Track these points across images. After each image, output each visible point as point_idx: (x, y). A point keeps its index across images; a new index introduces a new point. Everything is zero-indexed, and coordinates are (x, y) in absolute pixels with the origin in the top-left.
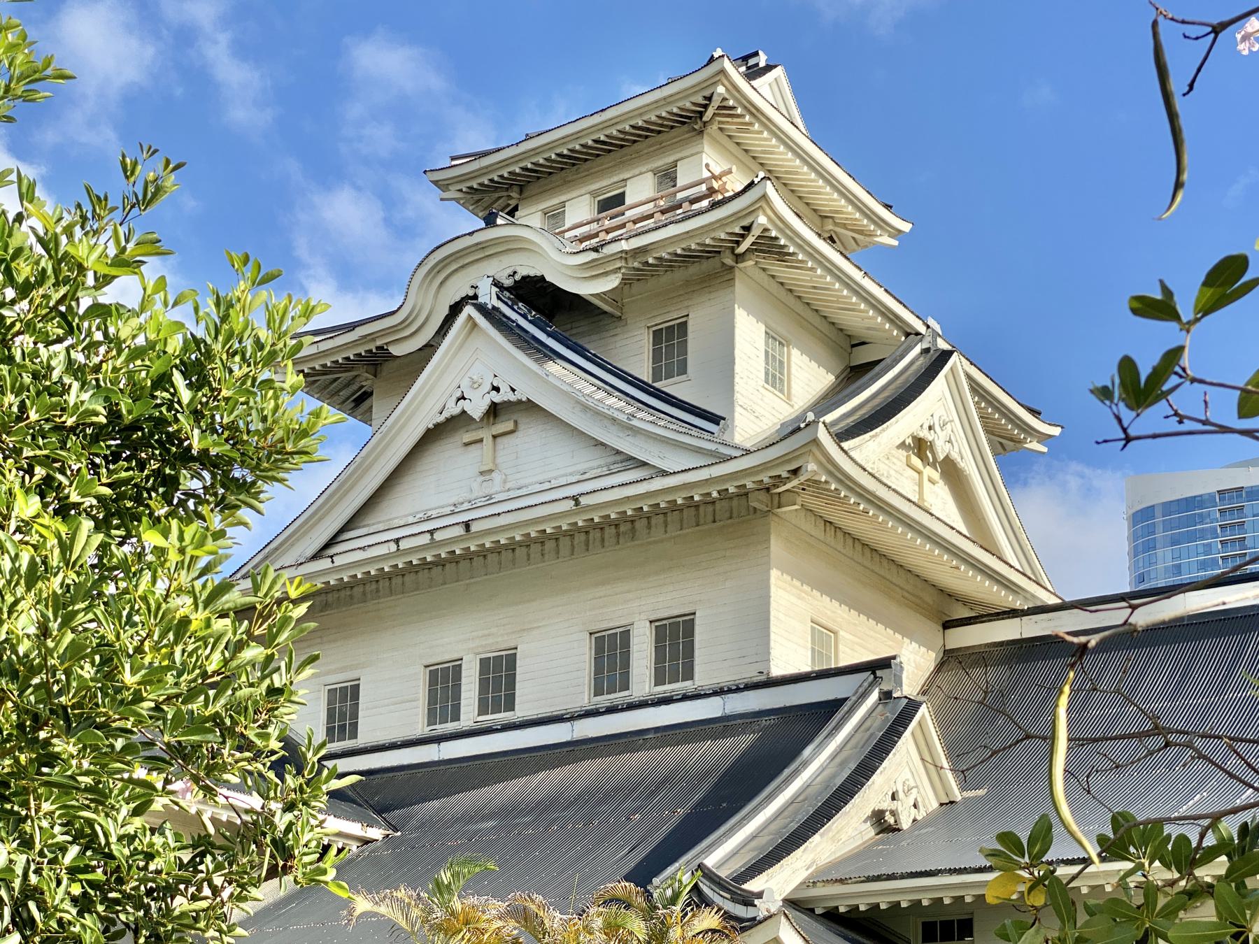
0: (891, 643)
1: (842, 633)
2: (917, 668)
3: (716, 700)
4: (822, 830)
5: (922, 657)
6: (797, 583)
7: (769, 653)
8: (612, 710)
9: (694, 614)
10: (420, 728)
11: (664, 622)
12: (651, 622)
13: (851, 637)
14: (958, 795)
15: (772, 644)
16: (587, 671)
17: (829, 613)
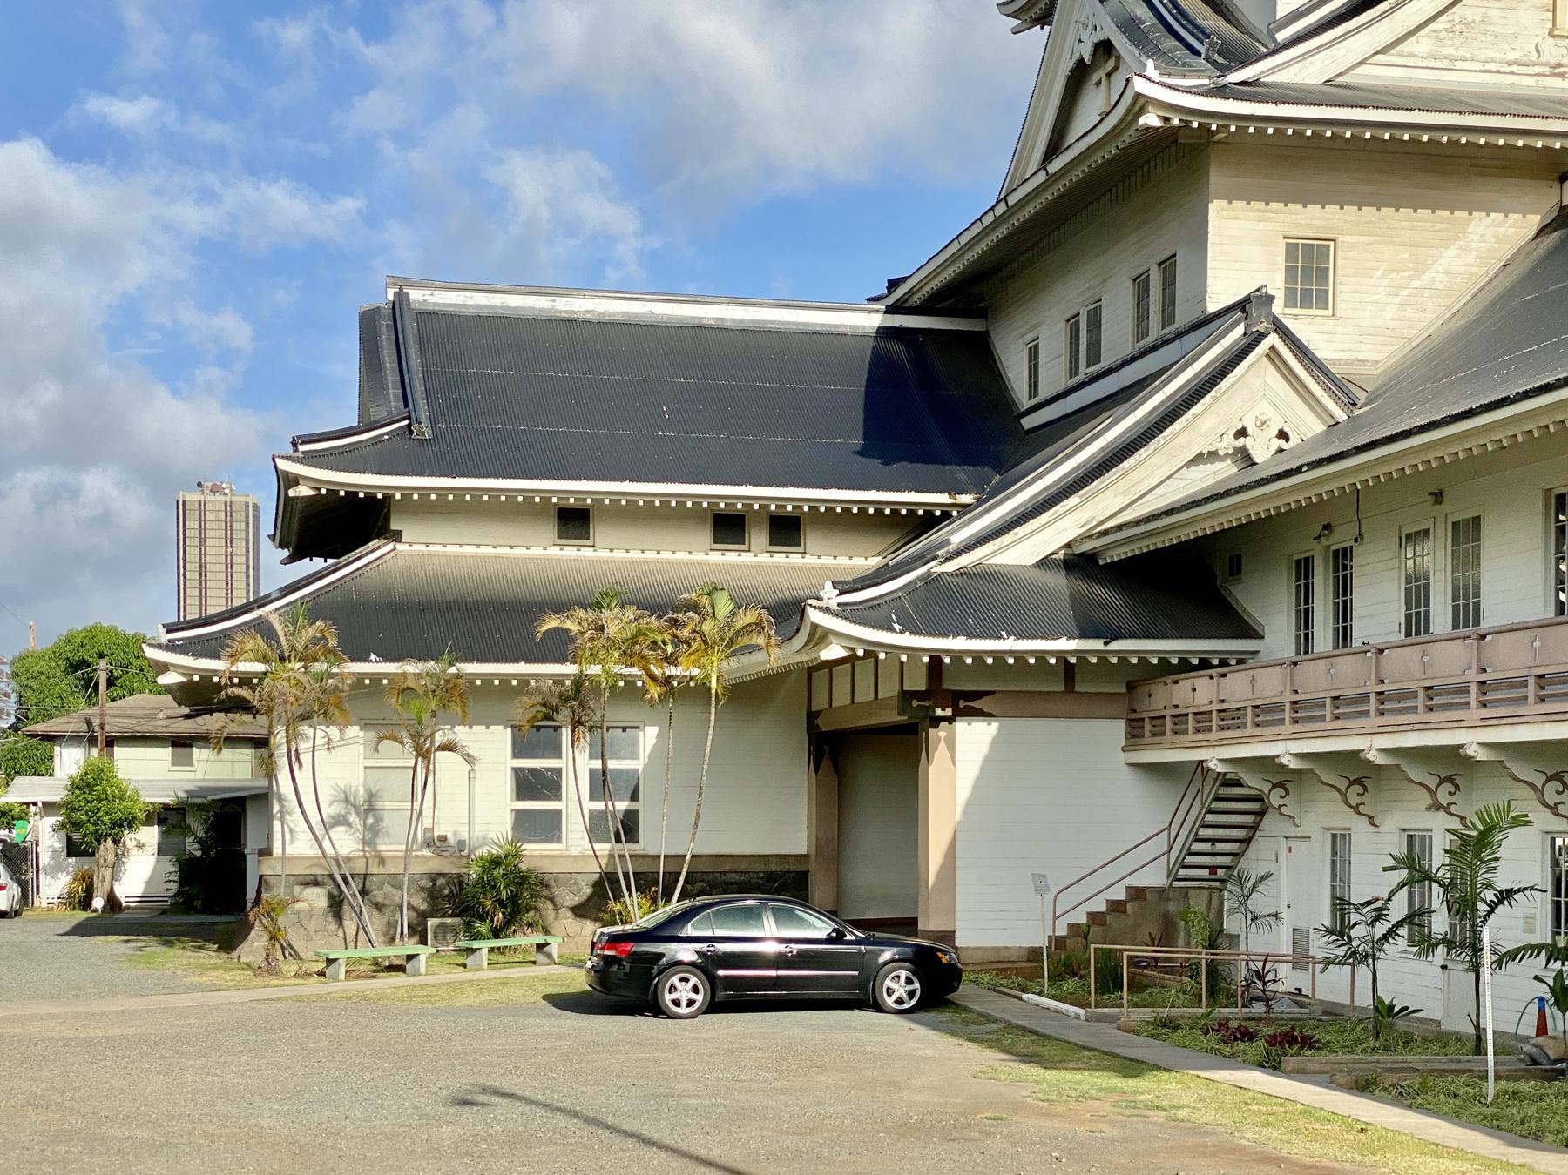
0: (1443, 226)
1: (1341, 239)
2: (1498, 240)
3: (1178, 342)
4: (1081, 492)
5: (1510, 226)
6: (1255, 205)
7: (1205, 292)
8: (1133, 359)
9: (1174, 255)
10: (1064, 383)
11: (1167, 264)
12: (1160, 265)
13: (1362, 239)
14: (1341, 416)
15: (1209, 281)
16: (1131, 318)
17: (1318, 222)
